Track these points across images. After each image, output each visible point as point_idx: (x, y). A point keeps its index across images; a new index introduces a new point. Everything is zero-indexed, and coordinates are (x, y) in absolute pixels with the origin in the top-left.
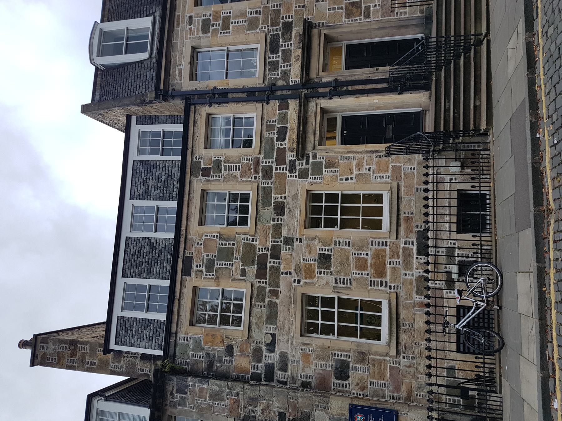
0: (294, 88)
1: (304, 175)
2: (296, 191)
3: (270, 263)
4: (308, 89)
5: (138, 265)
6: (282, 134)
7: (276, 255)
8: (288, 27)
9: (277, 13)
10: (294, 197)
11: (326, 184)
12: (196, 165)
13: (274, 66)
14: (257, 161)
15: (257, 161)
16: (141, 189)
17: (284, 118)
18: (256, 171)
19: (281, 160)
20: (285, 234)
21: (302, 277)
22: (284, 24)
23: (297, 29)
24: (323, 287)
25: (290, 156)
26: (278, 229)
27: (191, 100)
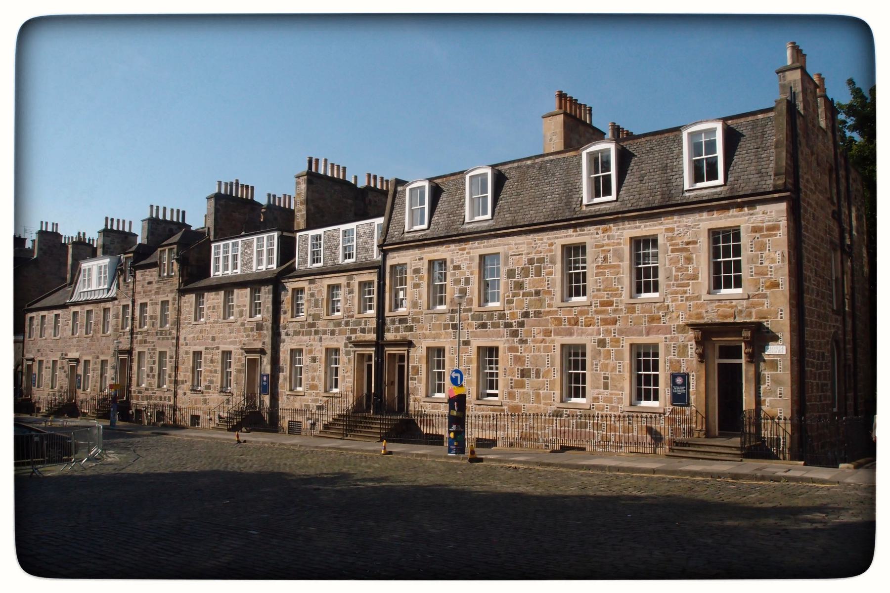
0: (383, 337)
1: (346, 346)
2: (339, 342)
3: (313, 329)
4: (380, 344)
5: (329, 241)
6: (363, 331)
7: (317, 332)
8: (411, 329)
9: (418, 321)
10: (337, 341)
11: (343, 358)
12: (350, 278)
13: (393, 322)
14: (352, 317)
15: (352, 317)
16: (362, 231)
17: (369, 332)
18: (348, 317)
19: (353, 331)
20: (324, 337)
21: (309, 348)
22: (412, 327)
23: (409, 335)
24: (306, 359)
25: (353, 336)
26: (325, 333)
27: (380, 268)
